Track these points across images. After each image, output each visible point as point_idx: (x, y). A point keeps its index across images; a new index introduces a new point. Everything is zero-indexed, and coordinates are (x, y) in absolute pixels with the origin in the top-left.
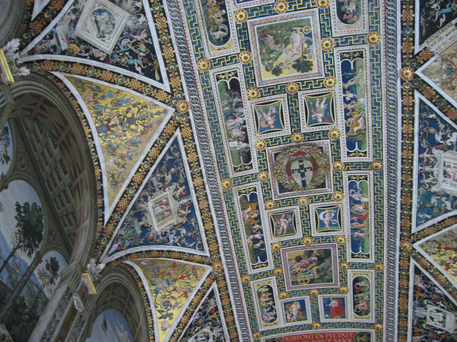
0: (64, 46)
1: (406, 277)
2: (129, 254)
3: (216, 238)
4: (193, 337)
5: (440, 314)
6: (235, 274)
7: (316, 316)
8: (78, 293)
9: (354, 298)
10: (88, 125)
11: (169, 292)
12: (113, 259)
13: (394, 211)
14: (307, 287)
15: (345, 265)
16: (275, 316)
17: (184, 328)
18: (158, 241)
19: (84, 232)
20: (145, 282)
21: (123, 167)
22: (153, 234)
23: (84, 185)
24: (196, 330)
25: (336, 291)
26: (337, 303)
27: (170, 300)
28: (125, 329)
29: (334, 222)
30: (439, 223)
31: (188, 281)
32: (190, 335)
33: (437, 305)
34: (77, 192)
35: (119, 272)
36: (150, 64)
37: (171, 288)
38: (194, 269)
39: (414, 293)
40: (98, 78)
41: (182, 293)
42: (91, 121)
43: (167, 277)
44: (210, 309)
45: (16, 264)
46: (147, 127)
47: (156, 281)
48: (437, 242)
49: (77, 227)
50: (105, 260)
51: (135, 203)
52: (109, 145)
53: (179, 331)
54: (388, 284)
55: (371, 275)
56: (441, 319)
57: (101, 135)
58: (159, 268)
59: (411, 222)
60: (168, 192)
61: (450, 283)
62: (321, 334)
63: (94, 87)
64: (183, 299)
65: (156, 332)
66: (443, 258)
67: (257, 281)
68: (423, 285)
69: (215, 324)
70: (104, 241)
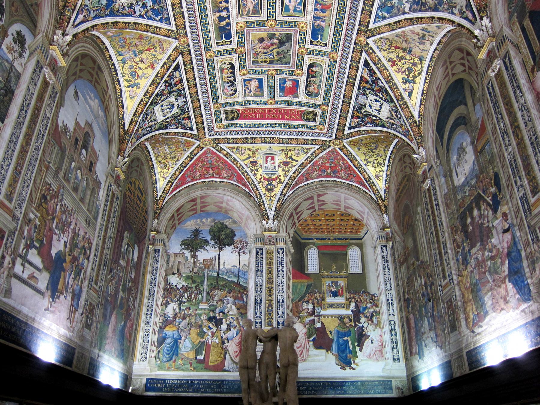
1: (356, 68)
2: (96, 26)
3: (183, 13)
4: (159, 105)
5: (378, 103)
6: (200, 49)
7: (272, 94)
8: (48, 65)
9: (307, 81)
11: (136, 63)
12: (80, 30)
13: (357, 5)
14: (266, 67)
15: (303, 50)
16: (235, 91)
17: (150, 97)
18: (124, 12)
20: (112, 52)
22: (119, 4)
24: (162, 99)
25: (292, 73)
26: (291, 84)
27: (137, 70)
28: (95, 98)
29: (299, 8)
30: (394, 23)
31: (154, 53)
32: (157, 104)
33: (377, 96)
35: (85, 42)
37: (138, 59)
38: (160, 42)
39: (360, 83)
41: (149, 64)
44: (175, 81)
47: (123, 52)
48: (389, 40)
50: (71, 31)
53: (146, 100)
54: (339, 73)
55: (325, 62)
56: (378, 108)
58: (125, 39)
59: (370, 18)
61: (392, 78)
62: (274, 109)
64: (150, 70)
65: (124, 99)
66: (391, 55)
67: (220, 57)
68: (369, 77)
69: (180, 94)
70: (68, 11)
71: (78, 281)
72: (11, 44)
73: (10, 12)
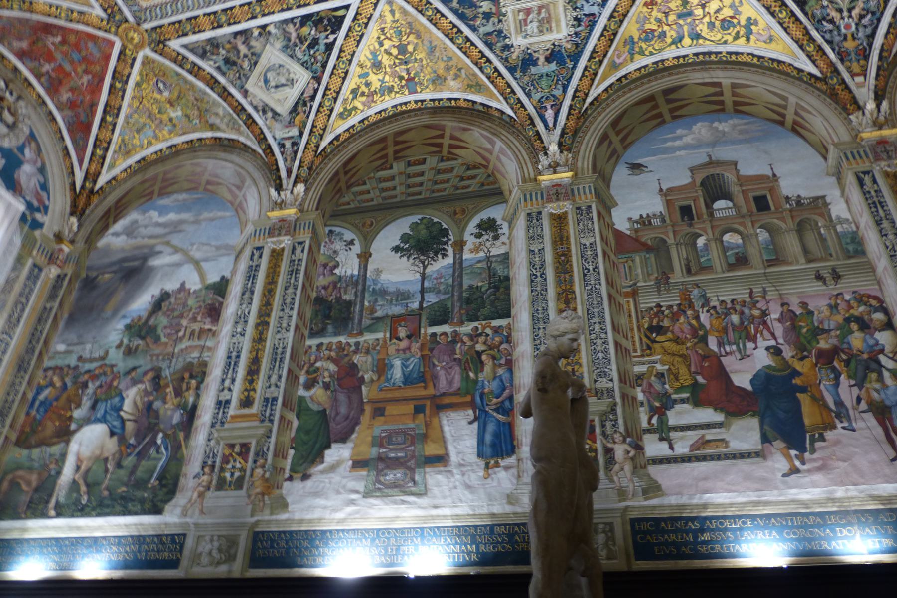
0: (294, 132)
10: (405, 104)
18: (583, 35)
19: (502, 157)
20: (670, 53)
21: (460, 70)
23: (458, 134)
27: (721, 17)
34: (454, 151)
35: (608, 105)
36: (326, 22)
37: (699, 12)
40: (338, 93)
42: (400, 99)
43: (672, 18)
45: (436, 278)
46: (411, 29)
49: (486, 167)
51: (506, 67)
52: (433, 81)
53: (783, 15)
57: (419, 90)
60: (509, 9)
63: (351, 97)
71: (880, 378)
72: (474, 243)
73: (456, 222)
